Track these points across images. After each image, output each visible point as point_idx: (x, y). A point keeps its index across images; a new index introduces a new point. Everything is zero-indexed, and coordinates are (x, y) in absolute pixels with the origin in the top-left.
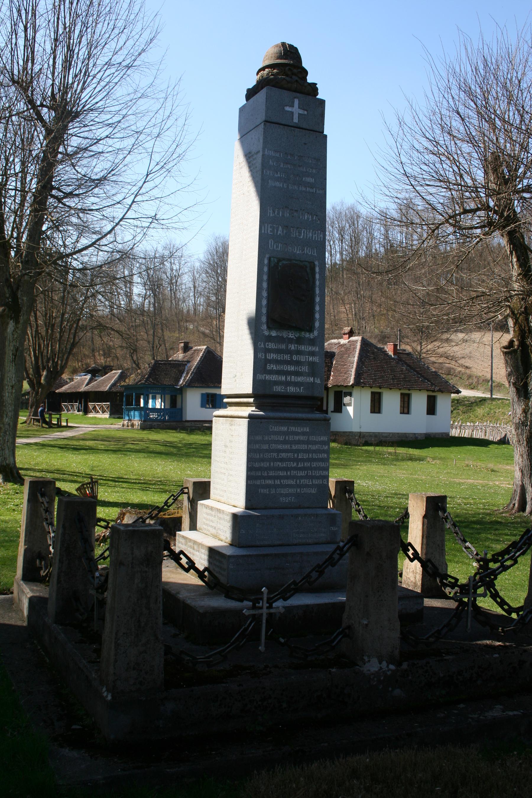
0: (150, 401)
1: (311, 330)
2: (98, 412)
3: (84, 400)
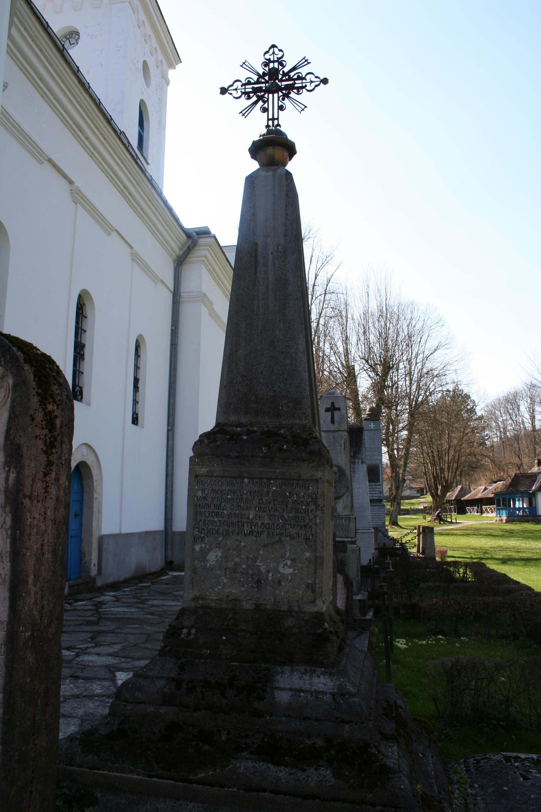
0: (517, 503)
1: (379, 482)
2: (489, 512)
3: (479, 503)
